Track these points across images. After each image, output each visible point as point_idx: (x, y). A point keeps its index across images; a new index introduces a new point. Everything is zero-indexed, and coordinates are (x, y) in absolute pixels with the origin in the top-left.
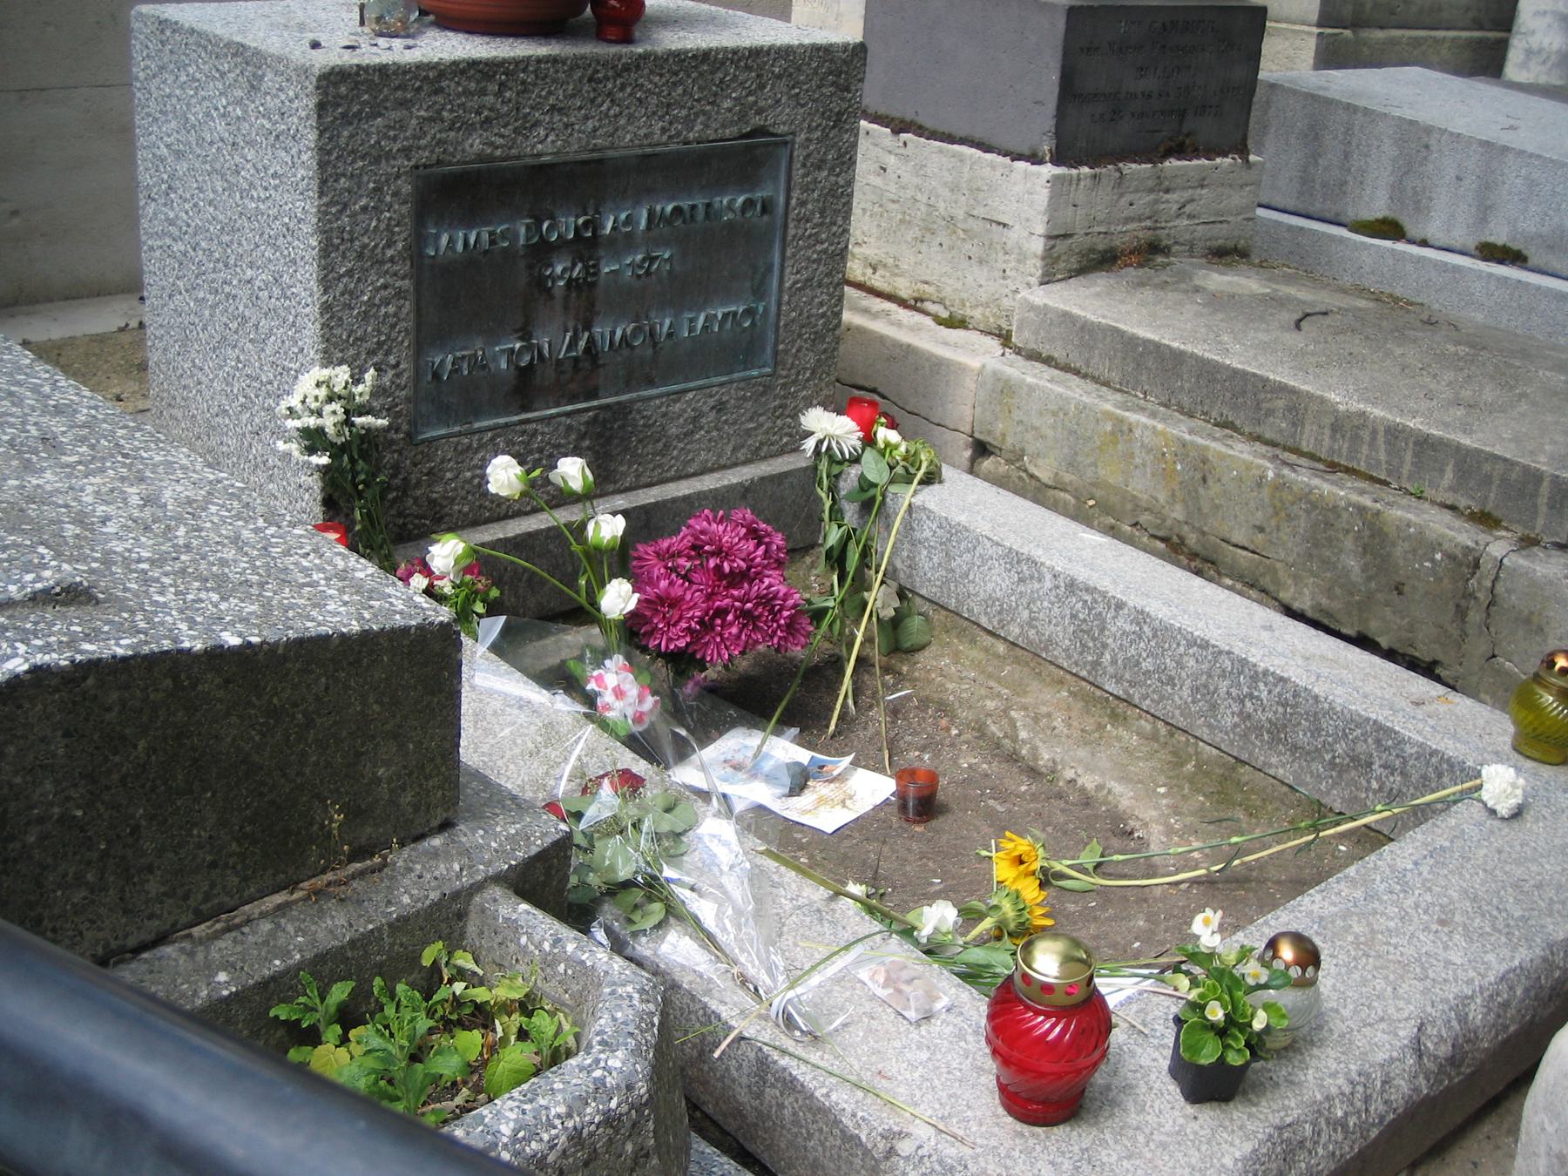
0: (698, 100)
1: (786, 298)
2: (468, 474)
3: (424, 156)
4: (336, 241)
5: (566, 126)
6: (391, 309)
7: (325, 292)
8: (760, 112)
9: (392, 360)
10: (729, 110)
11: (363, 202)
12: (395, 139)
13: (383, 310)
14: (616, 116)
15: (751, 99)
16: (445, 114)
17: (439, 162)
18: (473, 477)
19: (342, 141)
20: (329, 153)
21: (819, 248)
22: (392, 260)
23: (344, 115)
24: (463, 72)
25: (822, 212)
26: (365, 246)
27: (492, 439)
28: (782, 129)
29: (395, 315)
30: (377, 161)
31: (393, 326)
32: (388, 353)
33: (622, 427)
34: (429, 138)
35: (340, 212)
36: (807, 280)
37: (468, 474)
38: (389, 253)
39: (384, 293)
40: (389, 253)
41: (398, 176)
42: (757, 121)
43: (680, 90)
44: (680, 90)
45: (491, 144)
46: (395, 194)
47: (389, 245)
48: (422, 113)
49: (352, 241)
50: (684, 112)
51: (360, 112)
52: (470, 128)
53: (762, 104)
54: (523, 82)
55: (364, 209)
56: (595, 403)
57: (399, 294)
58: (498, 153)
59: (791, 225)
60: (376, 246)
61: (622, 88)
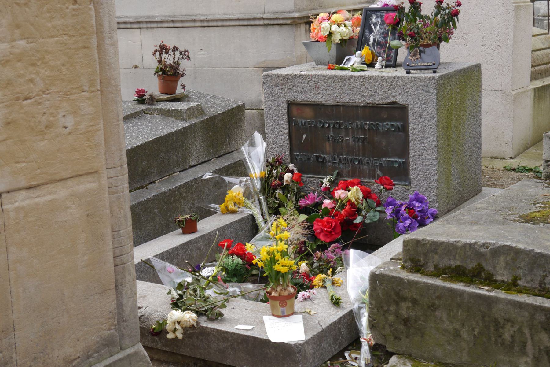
0: (370, 91)
3: (289, 98)
5: (328, 95)
6: (283, 137)
10: (382, 95)
12: (282, 93)
15: (389, 92)
21: (423, 145)
22: (283, 124)
23: (269, 86)
25: (423, 132)
26: (275, 119)
27: (313, 181)
30: (278, 98)
32: (283, 149)
36: (420, 155)
38: (282, 122)
40: (282, 122)
42: (393, 99)
46: (283, 107)
50: (366, 94)
51: (272, 85)
52: (301, 92)
53: (393, 94)
55: (275, 110)
59: (411, 135)
61: (344, 86)
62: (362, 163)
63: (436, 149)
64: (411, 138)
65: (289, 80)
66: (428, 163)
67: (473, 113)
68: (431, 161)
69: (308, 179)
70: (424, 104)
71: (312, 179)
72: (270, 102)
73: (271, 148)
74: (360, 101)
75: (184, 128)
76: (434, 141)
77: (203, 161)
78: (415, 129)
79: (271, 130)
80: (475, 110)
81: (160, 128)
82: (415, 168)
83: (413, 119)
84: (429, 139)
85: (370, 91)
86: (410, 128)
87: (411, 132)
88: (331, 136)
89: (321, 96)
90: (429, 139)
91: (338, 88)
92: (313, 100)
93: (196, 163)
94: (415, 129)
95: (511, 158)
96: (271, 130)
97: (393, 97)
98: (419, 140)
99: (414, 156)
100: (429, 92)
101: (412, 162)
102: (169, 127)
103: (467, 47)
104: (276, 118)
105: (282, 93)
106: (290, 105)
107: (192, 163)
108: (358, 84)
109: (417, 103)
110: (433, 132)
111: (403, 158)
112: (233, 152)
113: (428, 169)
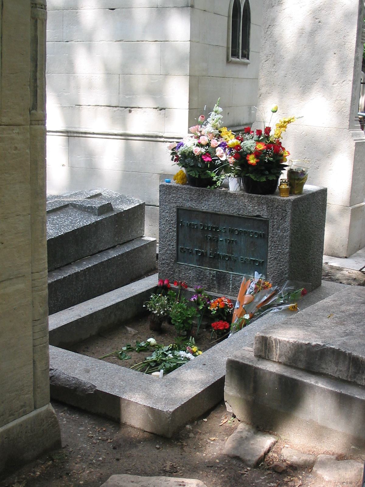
1: (269, 261)
2: (187, 275)
4: (162, 217)
7: (160, 226)
8: (258, 211)
9: (172, 244)
11: (167, 211)
12: (173, 200)
13: (170, 233)
14: (220, 205)
16: (183, 197)
17: (182, 206)
18: (188, 276)
19: (164, 198)
20: (161, 200)
24: (186, 189)
27: (192, 269)
28: (265, 217)
29: (173, 235)
30: (170, 203)
31: (172, 237)
32: (171, 242)
33: (223, 278)
34: (180, 201)
35: (163, 212)
36: (275, 258)
37: (187, 275)
38: (172, 222)
39: (170, 230)
40: (172, 222)
41: (174, 207)
43: (236, 202)
44: (236, 202)
45: (192, 205)
46: (173, 211)
47: (172, 220)
48: (178, 196)
49: (165, 218)
50: (237, 207)
51: (167, 193)
54: (199, 194)
55: (167, 212)
56: (217, 270)
57: (173, 231)
58: (194, 207)
59: (270, 242)
60: (169, 220)
62: (231, 260)
63: (288, 254)
64: (269, 244)
65: (179, 191)
66: (282, 265)
67: (319, 226)
68: (283, 263)
69: (189, 267)
70: (281, 220)
71: (192, 268)
72: (164, 206)
73: (162, 241)
74: (232, 212)
75: (96, 222)
76: (287, 248)
77: (110, 247)
78: (273, 238)
79: (163, 228)
80: (321, 224)
81: (78, 220)
82: (271, 267)
83: (273, 230)
84: (283, 247)
85: (241, 205)
86: (270, 236)
87: (269, 240)
88: (209, 237)
89: (203, 205)
90: (283, 247)
91: (216, 201)
92: (197, 208)
93: (105, 249)
94: (273, 238)
95: (346, 257)
96: (163, 228)
97: (257, 212)
98: (275, 247)
99: (271, 258)
100: (285, 211)
101: (269, 262)
102: (85, 221)
103: (318, 170)
104: (167, 219)
105: (173, 200)
106: (179, 210)
107: (101, 249)
108: (232, 199)
109: (276, 219)
110: (286, 241)
111: (262, 259)
112: (133, 240)
113: (281, 269)
